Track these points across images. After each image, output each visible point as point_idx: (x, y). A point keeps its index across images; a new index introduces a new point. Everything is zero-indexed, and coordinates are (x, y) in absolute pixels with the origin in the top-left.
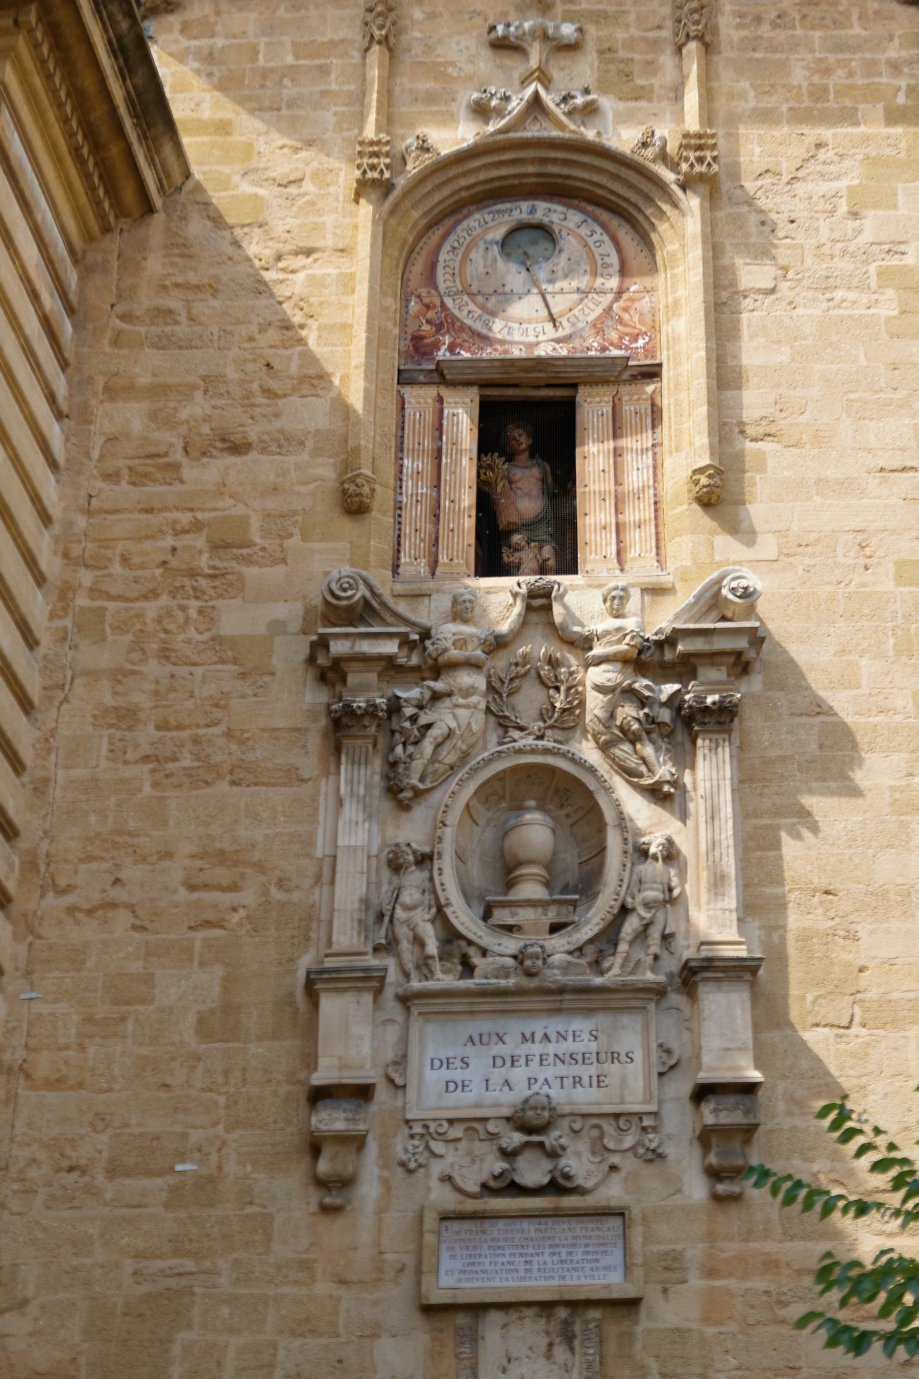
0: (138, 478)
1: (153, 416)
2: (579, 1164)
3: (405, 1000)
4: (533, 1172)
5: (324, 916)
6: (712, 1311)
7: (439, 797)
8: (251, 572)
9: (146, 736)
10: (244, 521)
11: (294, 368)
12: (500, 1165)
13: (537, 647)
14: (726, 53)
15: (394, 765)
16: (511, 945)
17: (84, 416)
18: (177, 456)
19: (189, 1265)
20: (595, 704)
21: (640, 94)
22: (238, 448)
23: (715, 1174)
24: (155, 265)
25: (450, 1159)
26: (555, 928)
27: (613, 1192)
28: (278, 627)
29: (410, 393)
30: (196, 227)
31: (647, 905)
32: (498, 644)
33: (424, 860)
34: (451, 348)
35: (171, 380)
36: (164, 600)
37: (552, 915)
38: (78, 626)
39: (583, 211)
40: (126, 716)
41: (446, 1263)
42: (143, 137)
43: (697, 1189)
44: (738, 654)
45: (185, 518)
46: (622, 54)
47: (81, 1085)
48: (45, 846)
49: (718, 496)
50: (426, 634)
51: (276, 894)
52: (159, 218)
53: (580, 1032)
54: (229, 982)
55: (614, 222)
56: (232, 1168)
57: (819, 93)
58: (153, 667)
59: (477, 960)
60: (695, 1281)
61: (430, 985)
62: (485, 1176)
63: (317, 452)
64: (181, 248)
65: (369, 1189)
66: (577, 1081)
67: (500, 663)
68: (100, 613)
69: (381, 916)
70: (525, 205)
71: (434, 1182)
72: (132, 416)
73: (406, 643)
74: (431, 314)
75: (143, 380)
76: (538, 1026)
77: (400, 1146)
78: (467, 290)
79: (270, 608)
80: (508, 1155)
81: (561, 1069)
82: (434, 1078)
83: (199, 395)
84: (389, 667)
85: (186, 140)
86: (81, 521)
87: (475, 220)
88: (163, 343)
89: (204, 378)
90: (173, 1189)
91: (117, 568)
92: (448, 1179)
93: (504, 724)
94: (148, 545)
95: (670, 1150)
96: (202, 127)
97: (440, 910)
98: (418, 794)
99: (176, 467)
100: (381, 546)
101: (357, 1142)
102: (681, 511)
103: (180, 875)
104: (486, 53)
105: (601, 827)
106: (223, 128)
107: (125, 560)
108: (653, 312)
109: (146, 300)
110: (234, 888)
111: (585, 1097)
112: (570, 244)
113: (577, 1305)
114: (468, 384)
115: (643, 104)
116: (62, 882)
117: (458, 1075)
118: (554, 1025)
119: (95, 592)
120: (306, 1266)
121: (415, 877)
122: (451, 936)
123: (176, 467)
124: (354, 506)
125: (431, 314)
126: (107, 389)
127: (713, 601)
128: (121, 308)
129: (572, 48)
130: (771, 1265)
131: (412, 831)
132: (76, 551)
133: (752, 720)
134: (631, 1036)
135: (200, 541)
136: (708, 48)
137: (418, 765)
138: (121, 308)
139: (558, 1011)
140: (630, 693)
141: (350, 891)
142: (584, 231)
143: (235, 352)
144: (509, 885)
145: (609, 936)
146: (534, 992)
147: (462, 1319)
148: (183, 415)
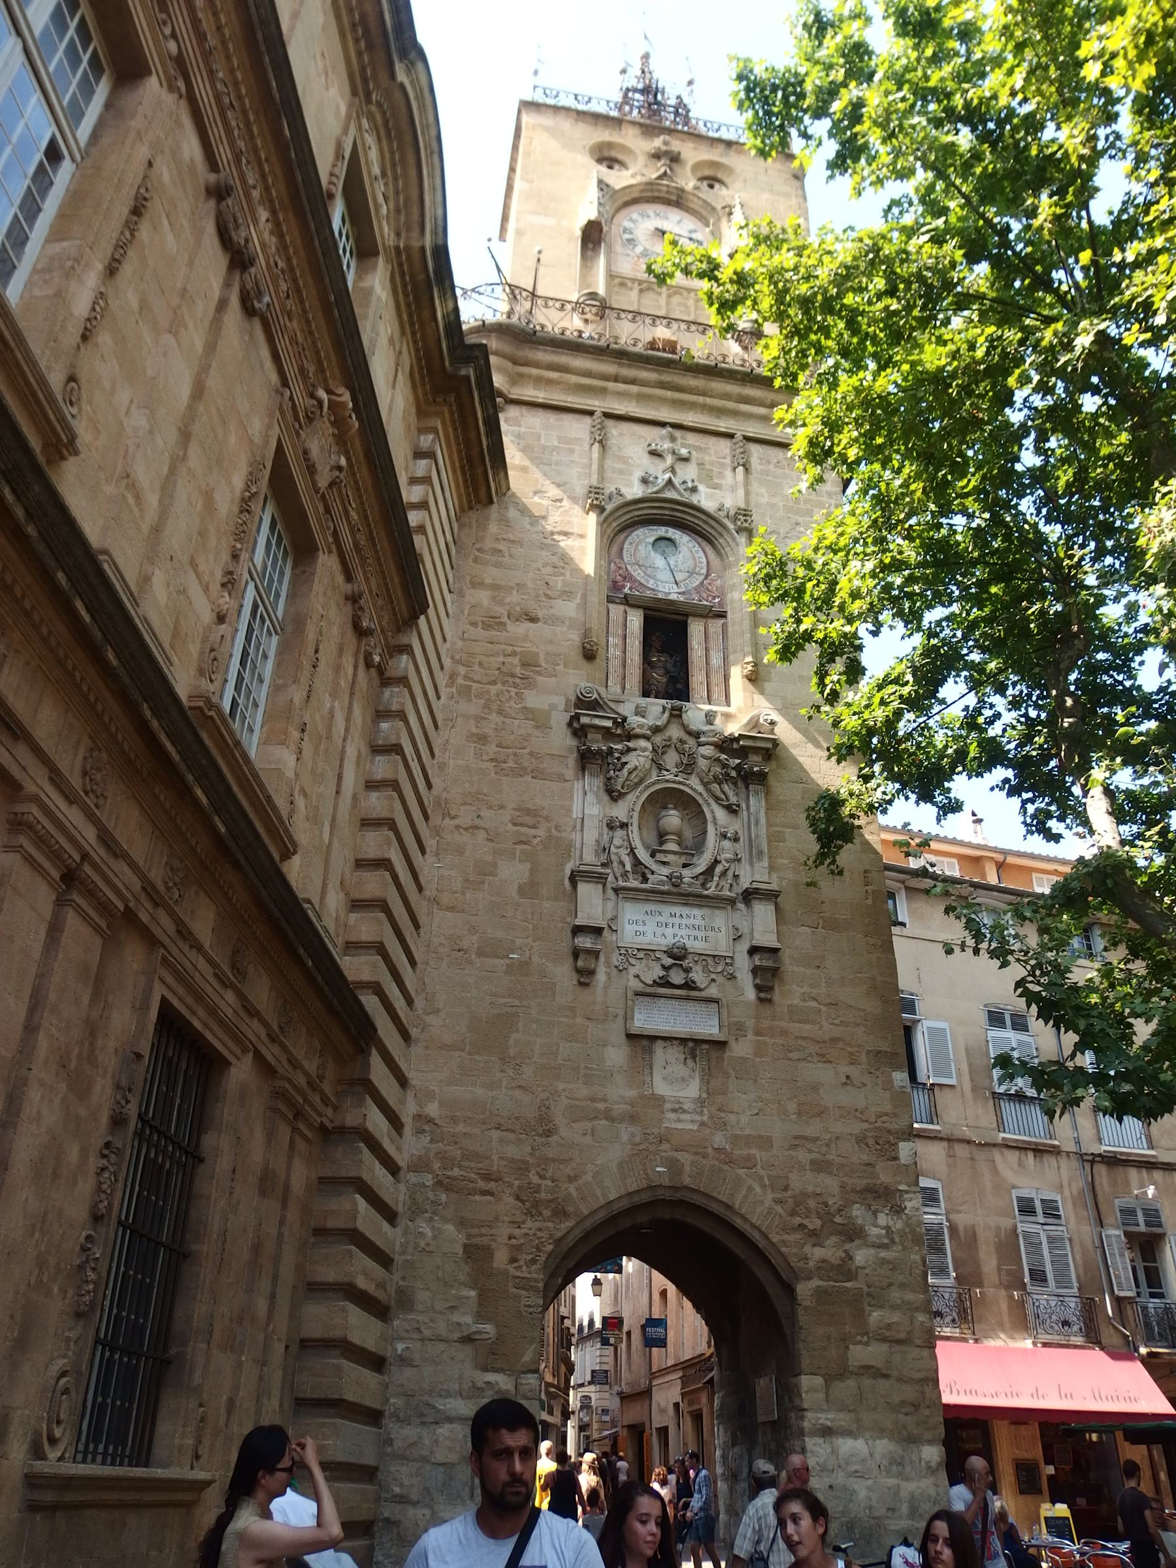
0: (487, 627)
1: (494, 598)
2: (698, 976)
3: (616, 890)
4: (677, 977)
5: (578, 845)
6: (759, 1050)
7: (631, 797)
8: (540, 679)
9: (491, 749)
10: (537, 654)
11: (559, 586)
12: (662, 973)
13: (675, 732)
14: (754, 475)
15: (609, 779)
16: (665, 871)
17: (461, 594)
18: (505, 619)
19: (517, 1002)
20: (702, 764)
21: (716, 487)
22: (534, 620)
23: (759, 988)
24: (493, 528)
25: (638, 968)
26: (685, 866)
27: (713, 991)
28: (553, 707)
29: (611, 606)
30: (512, 513)
31: (727, 861)
36: (499, 686)
37: (683, 860)
38: (459, 693)
40: (482, 739)
41: (637, 1016)
42: (492, 467)
43: (751, 994)
44: (767, 750)
45: (509, 649)
47: (463, 911)
48: (444, 795)
50: (625, 719)
51: (554, 832)
52: (495, 506)
53: (695, 916)
54: (532, 871)
55: (704, 544)
56: (535, 959)
58: (494, 717)
60: (750, 1036)
61: (628, 884)
62: (656, 977)
63: (570, 627)
64: (505, 522)
65: (601, 977)
66: (696, 938)
67: (658, 739)
68: (469, 688)
71: (631, 977)
72: (483, 597)
73: (615, 720)
75: (488, 581)
76: (677, 910)
77: (616, 959)
78: (637, 564)
79: (552, 698)
80: (666, 968)
81: (689, 932)
84: (607, 733)
85: (510, 473)
86: (460, 643)
87: (640, 532)
88: (497, 565)
90: (508, 966)
91: (476, 668)
92: (637, 976)
93: (660, 768)
94: (492, 659)
95: (738, 974)
96: (516, 468)
97: (632, 850)
98: (621, 795)
99: (504, 624)
101: (596, 954)
103: (508, 818)
104: (647, 455)
105: (705, 821)
106: (524, 469)
107: (480, 664)
108: (722, 587)
109: (489, 544)
110: (534, 827)
112: (684, 549)
113: (698, 1042)
114: (638, 607)
116: (453, 813)
117: (641, 928)
118: (685, 911)
119: (466, 678)
120: (572, 1009)
121: (620, 833)
122: (637, 863)
123: (504, 624)
124: (589, 655)
126: (471, 583)
127: (754, 723)
128: (478, 546)
129: (686, 460)
131: (620, 811)
132: (457, 657)
133: (772, 781)
134: (720, 919)
135: (516, 661)
137: (620, 781)
138: (478, 546)
139: (686, 904)
140: (718, 760)
141: (592, 834)
143: (531, 575)
144: (662, 843)
145: (709, 871)
146: (676, 894)
147: (645, 1042)
148: (508, 600)
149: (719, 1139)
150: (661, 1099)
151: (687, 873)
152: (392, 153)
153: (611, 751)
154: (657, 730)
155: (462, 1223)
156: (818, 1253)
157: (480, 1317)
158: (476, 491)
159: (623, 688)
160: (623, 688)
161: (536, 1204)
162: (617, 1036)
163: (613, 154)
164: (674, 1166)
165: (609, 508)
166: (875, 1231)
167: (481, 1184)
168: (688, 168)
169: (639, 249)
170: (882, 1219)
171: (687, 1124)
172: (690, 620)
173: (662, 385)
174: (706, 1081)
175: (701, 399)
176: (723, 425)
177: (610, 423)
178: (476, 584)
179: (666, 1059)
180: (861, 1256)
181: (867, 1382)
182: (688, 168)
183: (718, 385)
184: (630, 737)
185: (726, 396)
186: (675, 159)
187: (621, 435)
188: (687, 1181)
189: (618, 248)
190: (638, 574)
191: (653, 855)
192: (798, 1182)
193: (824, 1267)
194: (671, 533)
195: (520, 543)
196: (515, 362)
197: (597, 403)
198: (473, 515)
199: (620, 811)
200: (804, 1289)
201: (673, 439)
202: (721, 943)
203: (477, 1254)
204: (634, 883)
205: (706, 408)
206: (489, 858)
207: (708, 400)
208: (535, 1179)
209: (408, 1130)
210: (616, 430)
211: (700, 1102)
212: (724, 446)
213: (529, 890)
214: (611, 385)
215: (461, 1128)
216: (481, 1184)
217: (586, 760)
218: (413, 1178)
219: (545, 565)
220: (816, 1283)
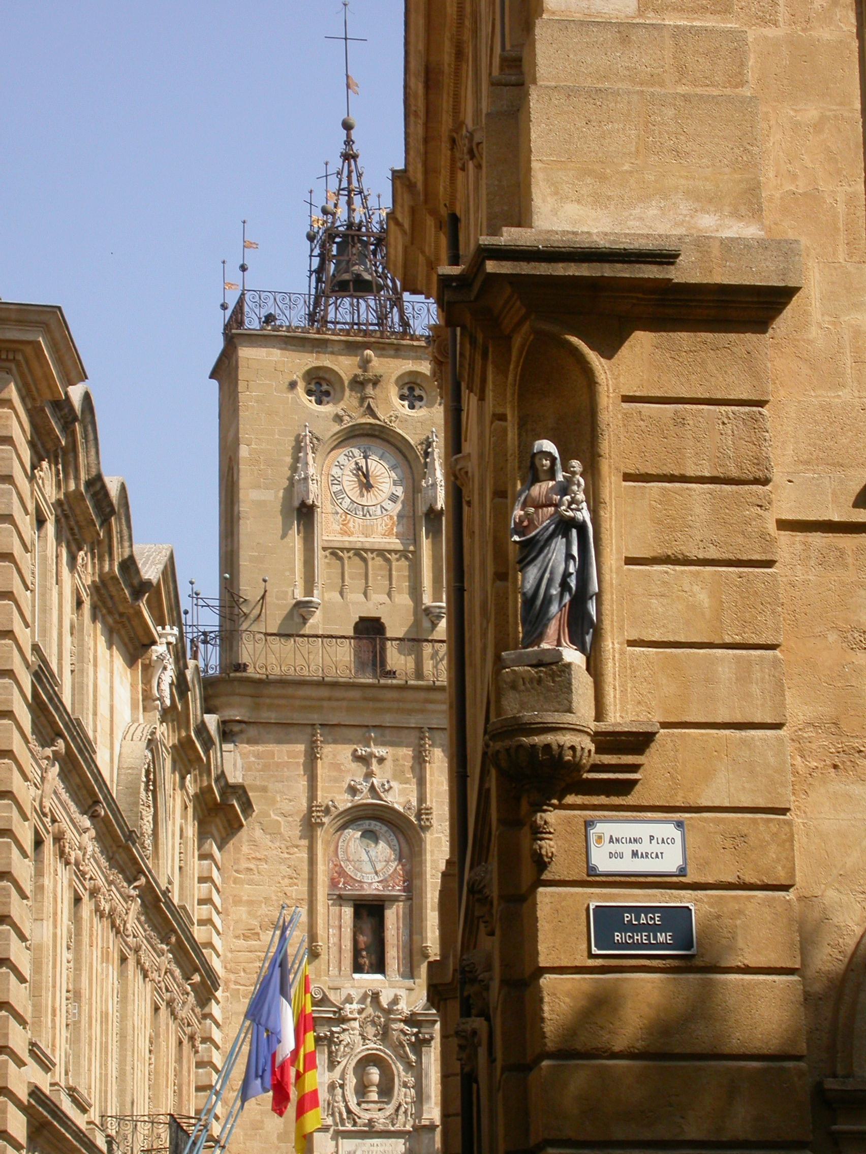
1: (249, 913)
16: (366, 1116)
24: (245, 849)
26: (380, 1110)
33: (342, 1086)
34: (344, 884)
35: (254, 899)
39: (386, 826)
46: (401, 762)
52: (245, 828)
59: (357, 1120)
67: (363, 1016)
69: (329, 1104)
70: (367, 822)
74: (337, 869)
75: (245, 898)
78: (348, 860)
83: (263, 905)
86: (229, 955)
88: (251, 882)
89: (265, 898)
91: (242, 974)
93: (364, 1038)
94: (251, 965)
99: (258, 934)
100: (324, 967)
107: (244, 970)
115: (408, 786)
119: (236, 983)
122: (349, 1111)
123: (258, 934)
125: (337, 869)
126: (234, 902)
128: (235, 868)
132: (229, 967)
137: (340, 1054)
142: (387, 835)
148: (259, 913)
153: (332, 1033)
154: (360, 1012)
159: (340, 970)
160: (340, 970)
172: (387, 903)
173: (365, 699)
176: (413, 722)
178: (237, 901)
184: (344, 1020)
190: (349, 869)
191: (359, 1104)
197: (316, 716)
204: (349, 1127)
206: (258, 1117)
207: (401, 705)
214: (325, 704)
219: (283, 877)
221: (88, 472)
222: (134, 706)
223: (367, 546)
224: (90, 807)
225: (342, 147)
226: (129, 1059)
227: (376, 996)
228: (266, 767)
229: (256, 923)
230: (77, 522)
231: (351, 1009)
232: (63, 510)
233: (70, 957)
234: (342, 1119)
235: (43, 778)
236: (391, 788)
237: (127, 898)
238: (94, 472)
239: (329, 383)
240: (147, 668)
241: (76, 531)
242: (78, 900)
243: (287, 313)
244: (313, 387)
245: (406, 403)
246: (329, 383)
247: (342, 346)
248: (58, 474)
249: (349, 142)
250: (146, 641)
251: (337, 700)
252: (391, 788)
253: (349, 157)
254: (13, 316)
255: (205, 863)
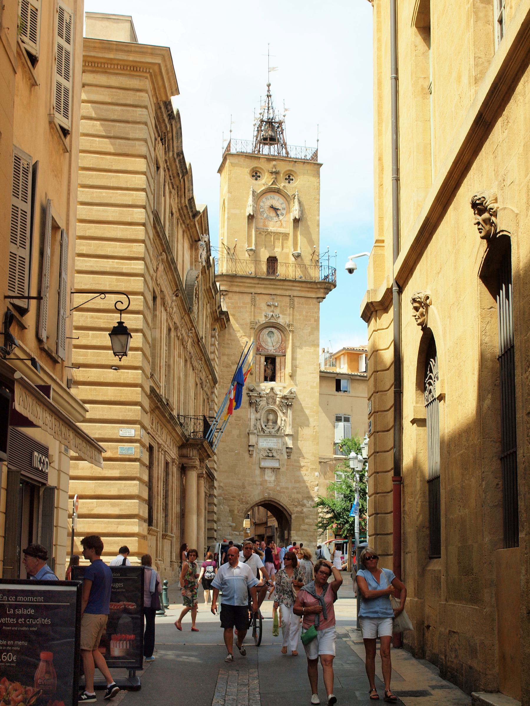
0: (227, 367)
2: (275, 454)
4: (270, 455)
6: (287, 469)
14: (296, 309)
18: (231, 364)
20: (277, 403)
23: (288, 456)
24: (227, 336)
27: (278, 457)
29: (257, 356)
30: (231, 331)
32: (267, 394)
33: (260, 419)
43: (286, 457)
49: (292, 376)
53: (275, 440)
57: (306, 316)
64: (230, 334)
65: (254, 455)
72: (225, 358)
75: (226, 353)
76: (271, 439)
82: (260, 444)
87: (265, 330)
88: (229, 348)
93: (268, 404)
100: (254, 378)
101: (253, 451)
102: (287, 377)
111: (275, 447)
112: (275, 335)
118: (273, 439)
119: (223, 382)
121: (259, 421)
122: (262, 428)
130: (293, 465)
131: (258, 416)
134: (280, 440)
136: (293, 308)
141: (253, 422)
144: (268, 422)
145: (278, 429)
149: (278, 488)
150: (267, 480)
151: (273, 430)
152: (209, 295)
155: (228, 506)
156: (297, 509)
157: (233, 522)
158: (222, 327)
161: (242, 502)
162: (257, 468)
163: (257, 170)
164: (269, 494)
165: (256, 327)
166: (308, 505)
167: (232, 499)
168: (282, 175)
169: (265, 215)
170: (310, 502)
171: (272, 485)
173: (271, 284)
174: (276, 476)
175: (281, 287)
176: (288, 293)
177: (256, 295)
179: (268, 473)
180: (305, 510)
181: (304, 532)
182: (282, 175)
183: (286, 283)
184: (261, 397)
185: (289, 286)
186: (277, 173)
187: (259, 299)
188: (271, 496)
189: (259, 217)
191: (266, 426)
192: (293, 496)
193: (297, 512)
194: (273, 330)
195: (234, 340)
196: (230, 282)
198: (222, 332)
199: (258, 416)
200: (293, 516)
201: (273, 299)
202: (280, 446)
203: (231, 511)
205: (282, 289)
207: (284, 287)
208: (242, 497)
209: (217, 488)
210: (258, 298)
211: (275, 481)
212: (288, 299)
213: (239, 436)
214: (257, 285)
215: (227, 488)
216: (232, 499)
217: (251, 404)
218: (219, 498)
220: (295, 515)
221: (177, 149)
222: (191, 264)
223: (273, 231)
224: (175, 292)
225: (266, 93)
226: (187, 397)
227: (272, 389)
228: (235, 308)
229: (230, 362)
230: (173, 174)
231: (263, 393)
232: (167, 166)
233: (167, 349)
234: (259, 431)
235: (157, 268)
236: (279, 317)
237: (188, 336)
238: (180, 149)
239: (260, 173)
240: (197, 249)
241: (172, 178)
242: (170, 330)
243: (246, 147)
244: (254, 174)
245: (287, 181)
246: (260, 173)
247: (266, 160)
248: (165, 149)
249: (269, 91)
250: (197, 239)
251: (261, 284)
252: (279, 317)
253: (269, 96)
254: (149, 51)
255: (213, 339)
